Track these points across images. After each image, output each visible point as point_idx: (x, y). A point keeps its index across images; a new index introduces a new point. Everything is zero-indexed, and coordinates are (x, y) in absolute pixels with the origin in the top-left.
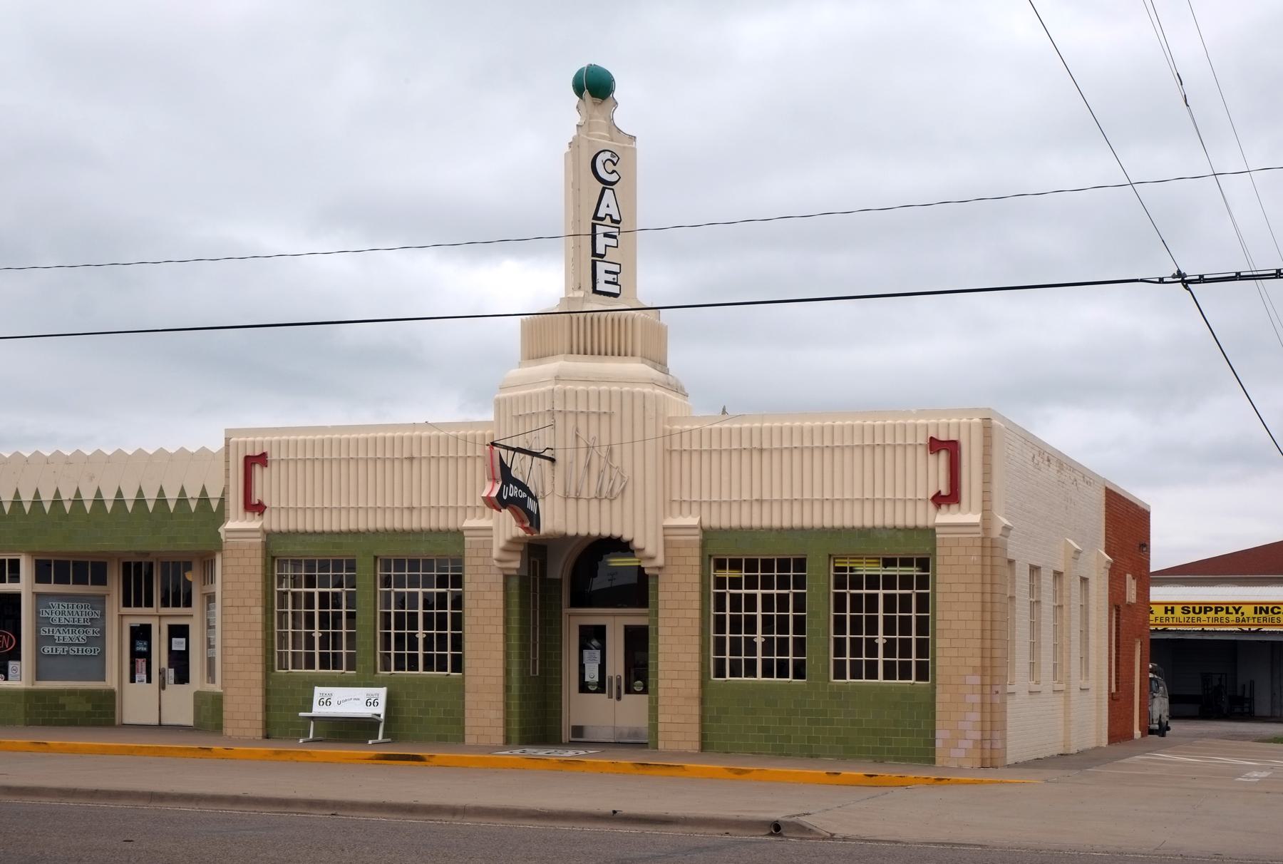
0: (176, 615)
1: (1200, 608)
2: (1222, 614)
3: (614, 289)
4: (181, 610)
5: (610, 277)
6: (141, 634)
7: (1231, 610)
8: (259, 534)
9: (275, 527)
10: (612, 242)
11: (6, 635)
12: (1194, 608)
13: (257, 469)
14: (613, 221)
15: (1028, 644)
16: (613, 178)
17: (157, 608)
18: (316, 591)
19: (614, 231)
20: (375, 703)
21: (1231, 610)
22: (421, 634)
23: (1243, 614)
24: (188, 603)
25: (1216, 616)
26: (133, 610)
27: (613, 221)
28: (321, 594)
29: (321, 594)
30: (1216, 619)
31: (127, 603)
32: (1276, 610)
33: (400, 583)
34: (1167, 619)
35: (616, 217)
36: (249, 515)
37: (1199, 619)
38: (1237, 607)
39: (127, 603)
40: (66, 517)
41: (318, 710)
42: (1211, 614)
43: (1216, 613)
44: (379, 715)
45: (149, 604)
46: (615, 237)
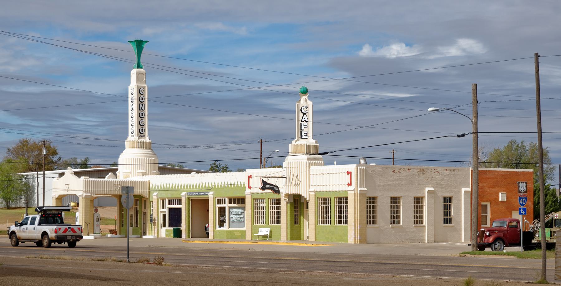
3: (307, 137)
5: (305, 134)
8: (250, 194)
10: (306, 126)
13: (250, 178)
14: (306, 122)
16: (306, 112)
19: (306, 124)
22: (276, 216)
27: (306, 122)
35: (307, 121)
41: (260, 233)
44: (268, 234)
46: (307, 125)
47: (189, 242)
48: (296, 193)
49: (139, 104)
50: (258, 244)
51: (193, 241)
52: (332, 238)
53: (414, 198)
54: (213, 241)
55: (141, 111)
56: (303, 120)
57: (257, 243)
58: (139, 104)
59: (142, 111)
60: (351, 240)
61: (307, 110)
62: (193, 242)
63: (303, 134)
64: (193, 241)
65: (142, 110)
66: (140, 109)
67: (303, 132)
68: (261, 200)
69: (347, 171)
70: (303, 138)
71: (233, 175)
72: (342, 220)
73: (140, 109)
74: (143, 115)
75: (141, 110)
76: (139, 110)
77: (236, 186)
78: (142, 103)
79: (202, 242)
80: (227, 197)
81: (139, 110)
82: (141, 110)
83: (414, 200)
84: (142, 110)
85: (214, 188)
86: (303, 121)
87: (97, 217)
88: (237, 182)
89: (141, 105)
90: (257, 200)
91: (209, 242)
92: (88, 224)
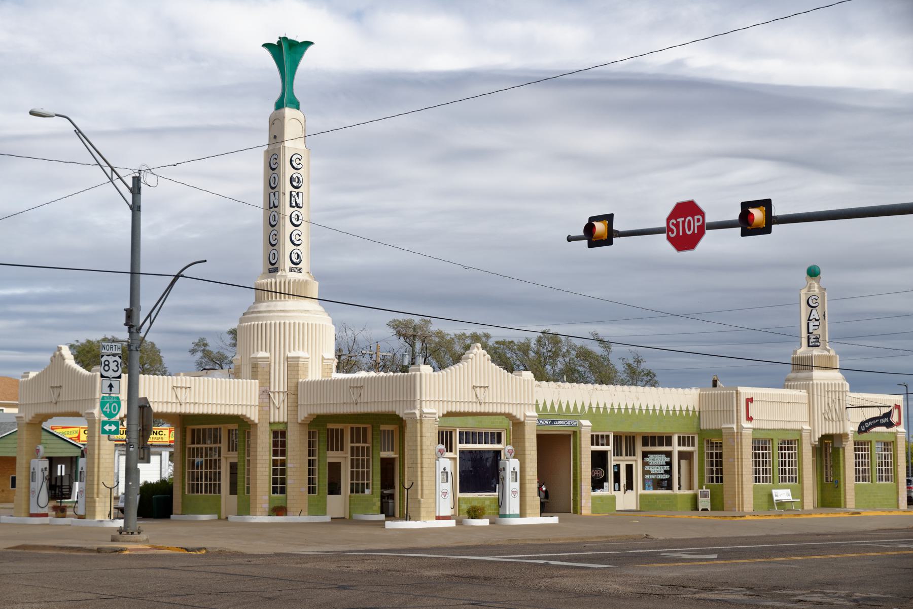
0: (629, 460)
4: (632, 458)
9: (755, 427)
11: (599, 469)
15: (724, 466)
16: (817, 304)
17: (624, 457)
20: (789, 495)
28: (716, 453)
29: (716, 453)
35: (817, 318)
36: (747, 421)
45: (621, 455)
47: (734, 519)
49: (291, 192)
50: (861, 516)
51: (743, 516)
52: (874, 502)
54: (781, 515)
55: (296, 208)
56: (810, 319)
57: (859, 513)
59: (298, 209)
60: (903, 505)
61: (816, 301)
62: (743, 519)
63: (811, 340)
64: (743, 516)
65: (298, 207)
66: (294, 204)
68: (793, 442)
69: (896, 405)
70: (812, 346)
71: (630, 392)
74: (298, 220)
76: (291, 206)
78: (297, 190)
79: (762, 516)
80: (614, 433)
81: (291, 206)
83: (855, 445)
85: (594, 415)
86: (811, 320)
88: (661, 406)
91: (775, 516)
92: (111, 489)
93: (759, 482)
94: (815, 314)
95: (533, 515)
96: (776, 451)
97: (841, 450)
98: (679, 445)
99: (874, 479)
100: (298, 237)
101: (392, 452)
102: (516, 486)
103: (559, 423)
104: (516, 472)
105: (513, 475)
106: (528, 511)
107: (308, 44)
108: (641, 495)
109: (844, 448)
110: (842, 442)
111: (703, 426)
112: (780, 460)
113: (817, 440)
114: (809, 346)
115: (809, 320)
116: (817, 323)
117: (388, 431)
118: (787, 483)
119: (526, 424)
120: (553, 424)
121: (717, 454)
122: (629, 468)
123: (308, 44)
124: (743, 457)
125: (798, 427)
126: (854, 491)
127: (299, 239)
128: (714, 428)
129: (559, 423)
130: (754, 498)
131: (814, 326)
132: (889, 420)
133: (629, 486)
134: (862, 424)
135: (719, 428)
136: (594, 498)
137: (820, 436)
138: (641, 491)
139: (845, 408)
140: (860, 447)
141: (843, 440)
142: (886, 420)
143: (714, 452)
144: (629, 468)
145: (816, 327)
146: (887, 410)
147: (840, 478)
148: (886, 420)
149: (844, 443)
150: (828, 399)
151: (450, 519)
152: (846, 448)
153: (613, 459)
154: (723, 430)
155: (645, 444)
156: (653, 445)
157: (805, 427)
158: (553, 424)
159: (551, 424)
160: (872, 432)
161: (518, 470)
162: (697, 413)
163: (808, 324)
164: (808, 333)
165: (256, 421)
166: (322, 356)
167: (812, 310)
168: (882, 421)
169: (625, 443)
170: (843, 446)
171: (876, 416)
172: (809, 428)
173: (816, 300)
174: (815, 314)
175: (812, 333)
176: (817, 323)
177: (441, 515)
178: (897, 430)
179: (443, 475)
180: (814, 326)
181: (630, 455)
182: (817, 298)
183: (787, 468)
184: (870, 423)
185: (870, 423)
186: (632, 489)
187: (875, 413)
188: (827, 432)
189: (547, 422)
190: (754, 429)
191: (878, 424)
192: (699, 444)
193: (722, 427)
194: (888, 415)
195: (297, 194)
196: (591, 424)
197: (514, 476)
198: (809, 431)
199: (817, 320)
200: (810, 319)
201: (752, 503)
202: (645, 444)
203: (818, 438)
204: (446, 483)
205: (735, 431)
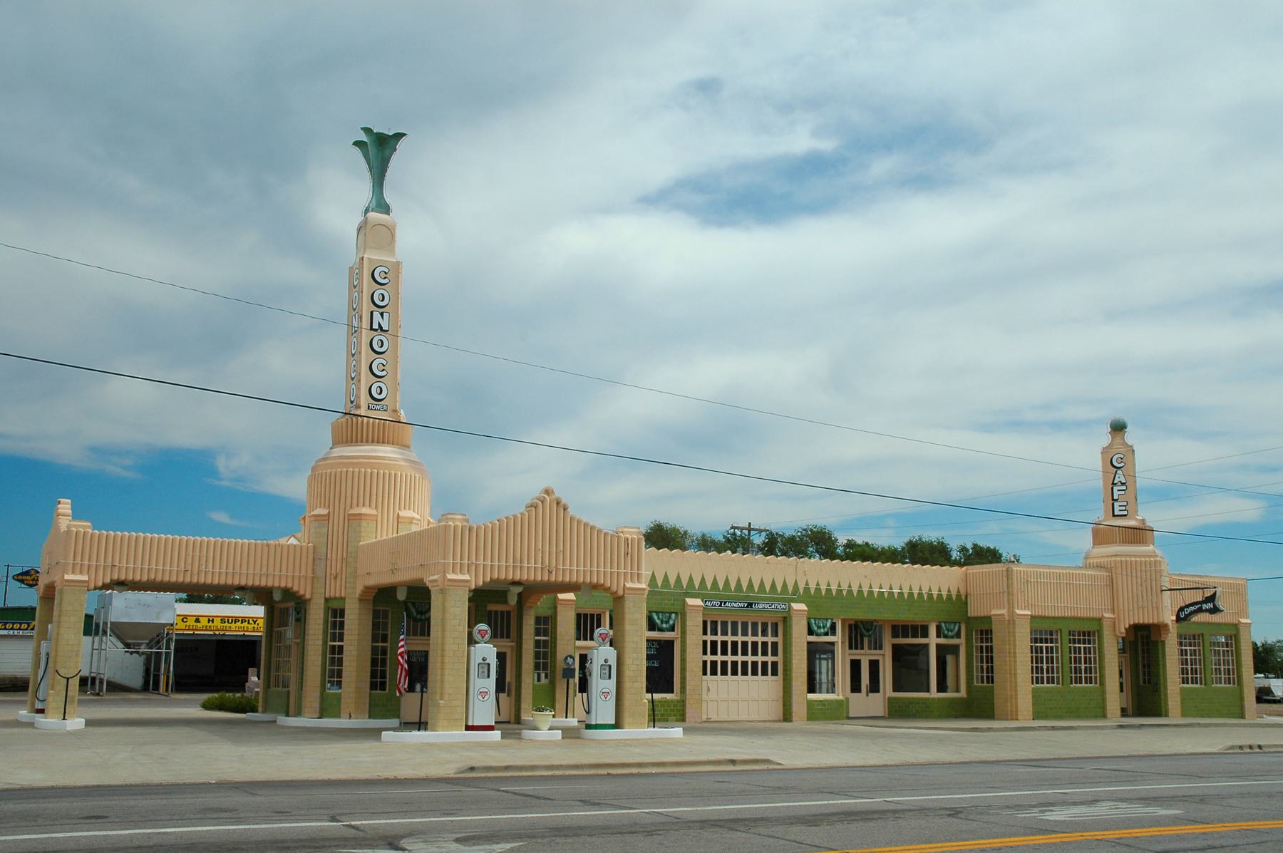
0: (874, 654)
1: (232, 620)
2: (245, 624)
3: (1125, 513)
4: (878, 652)
6: (855, 665)
7: (251, 622)
12: (228, 620)
16: (1122, 464)
17: (866, 650)
18: (984, 645)
21: (251, 622)
22: (1083, 666)
23: (258, 624)
24: (881, 648)
25: (242, 625)
26: (854, 651)
30: (241, 628)
31: (851, 648)
32: (185, 620)
33: (1074, 643)
34: (210, 627)
37: (230, 627)
38: (255, 620)
39: (851, 648)
40: (863, 599)
42: (239, 624)
43: (242, 623)
48: (1141, 622)
49: (372, 313)
53: (1070, 632)
56: (1115, 482)
58: (372, 313)
65: (382, 330)
66: (375, 326)
67: (1116, 504)
72: (1045, 675)
73: (375, 326)
74: (382, 346)
75: (376, 330)
76: (371, 329)
77: (886, 596)
78: (381, 310)
81: (371, 329)
82: (376, 330)
84: (382, 330)
86: (1116, 484)
87: (484, 659)
89: (377, 316)
90: (1231, 637)
93: (1081, 683)
94: (1120, 477)
95: (639, 725)
96: (1067, 645)
97: (1160, 644)
98: (938, 636)
99: (1209, 681)
100: (381, 367)
101: (508, 640)
102: (611, 685)
103: (760, 606)
104: (610, 666)
105: (605, 669)
106: (627, 719)
107: (399, 136)
108: (889, 699)
109: (1163, 642)
110: (1161, 635)
111: (971, 613)
112: (1073, 655)
113: (1123, 631)
114: (1114, 515)
115: (1113, 484)
116: (1124, 488)
117: (502, 612)
118: (1084, 684)
119: (626, 599)
120: (752, 607)
121: (987, 647)
122: (874, 665)
123: (399, 136)
124: (1017, 651)
125: (1098, 615)
126: (1179, 696)
127: (383, 370)
128: (982, 615)
129: (760, 606)
130: (1034, 704)
131: (1118, 490)
132: (1214, 605)
133: (874, 687)
134: (1181, 609)
135: (989, 615)
136: (810, 703)
137: (1127, 626)
138: (890, 693)
139: (1159, 591)
140: (1188, 641)
141: (1162, 632)
142: (1210, 606)
143: (984, 645)
144: (874, 665)
145: (1123, 492)
146: (1208, 593)
147: (1159, 680)
148: (1210, 606)
149: (1163, 636)
150: (1137, 580)
151: (493, 730)
152: (1166, 642)
153: (847, 653)
154: (992, 617)
155: (895, 635)
156: (906, 636)
157: (1106, 615)
158: (752, 607)
159: (747, 607)
160: (1194, 623)
161: (613, 663)
162: (963, 597)
163: (1112, 488)
164: (1113, 499)
165: (308, 596)
166: (398, 514)
167: (1116, 472)
168: (1205, 606)
169: (859, 633)
170: (1162, 639)
171: (1198, 600)
172: (1112, 616)
173: (1122, 459)
174: (1120, 477)
175: (1117, 500)
176: (1124, 488)
177: (475, 724)
178: (1239, 621)
179: (483, 668)
180: (1118, 490)
181: (856, 648)
182: (1122, 456)
183: (1083, 666)
184: (1192, 609)
185: (1192, 609)
186: (878, 691)
187: (1198, 596)
188: (1136, 622)
189: (740, 605)
190: (1032, 617)
191: (1200, 610)
192: (967, 635)
193: (992, 613)
194: (1212, 598)
195: (382, 314)
196: (806, 609)
197: (607, 671)
198: (1113, 620)
199: (1123, 484)
200: (1115, 482)
201: (1031, 709)
202: (895, 635)
203: (1126, 629)
204: (487, 680)
205: (1007, 618)
